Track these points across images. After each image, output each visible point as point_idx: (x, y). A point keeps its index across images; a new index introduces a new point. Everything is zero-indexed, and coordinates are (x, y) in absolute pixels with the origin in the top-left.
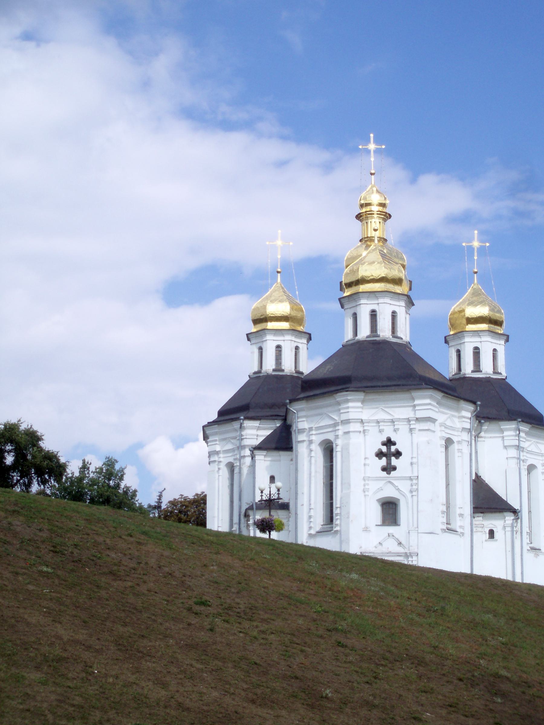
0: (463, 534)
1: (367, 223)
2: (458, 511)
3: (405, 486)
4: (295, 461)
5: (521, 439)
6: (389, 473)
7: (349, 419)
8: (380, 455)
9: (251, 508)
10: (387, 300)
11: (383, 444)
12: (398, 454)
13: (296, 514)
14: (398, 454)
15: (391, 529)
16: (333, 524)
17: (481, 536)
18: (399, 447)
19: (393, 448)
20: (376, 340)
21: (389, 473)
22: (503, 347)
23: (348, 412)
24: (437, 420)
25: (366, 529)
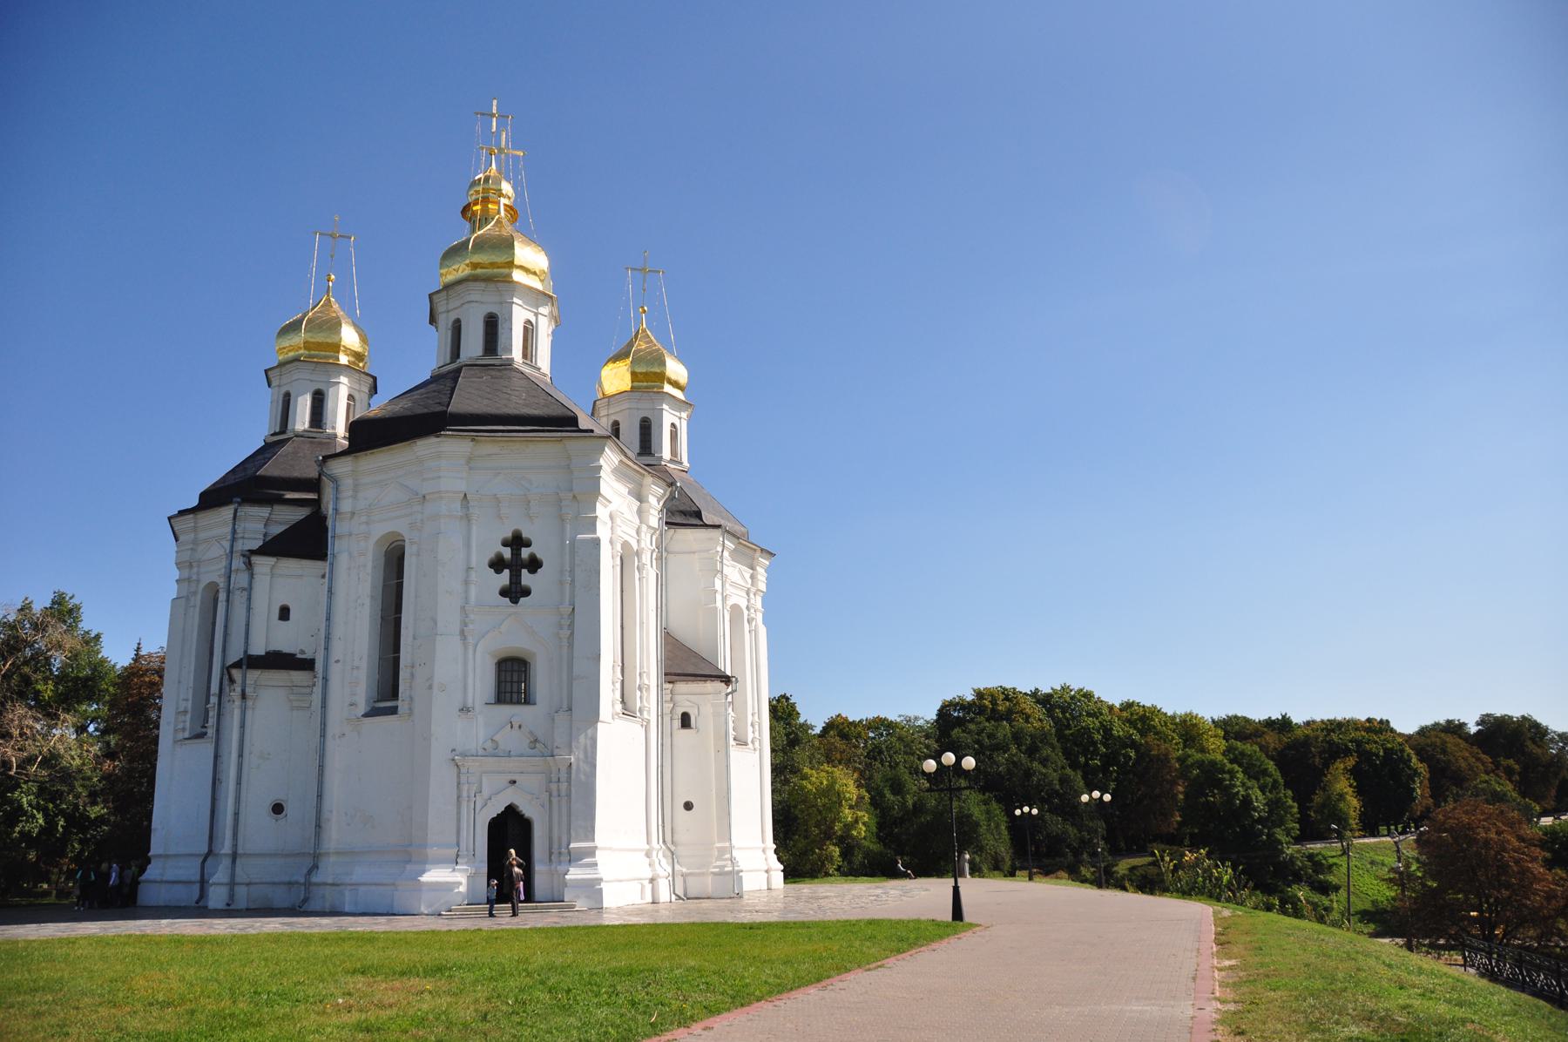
4: (330, 578)
5: (725, 561)
6: (515, 601)
7: (439, 492)
8: (497, 564)
9: (238, 665)
12: (534, 565)
13: (325, 679)
14: (534, 565)
16: (398, 699)
18: (537, 549)
19: (525, 553)
21: (515, 601)
22: (684, 423)
23: (439, 477)
24: (610, 502)
25: (465, 710)
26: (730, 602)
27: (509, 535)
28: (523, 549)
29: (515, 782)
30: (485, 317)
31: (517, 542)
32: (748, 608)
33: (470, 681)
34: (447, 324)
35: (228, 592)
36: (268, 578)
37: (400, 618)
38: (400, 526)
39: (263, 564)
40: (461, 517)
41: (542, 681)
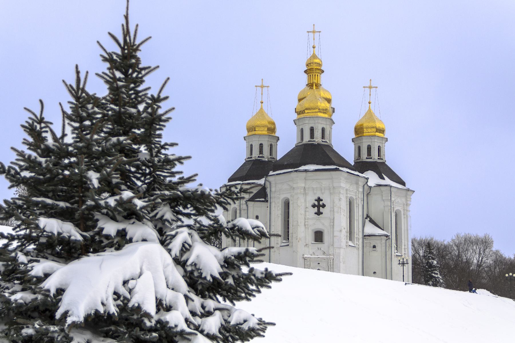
0: (359, 248)
1: (310, 75)
2: (356, 236)
3: (327, 223)
8: (314, 206)
10: (320, 121)
11: (316, 200)
14: (324, 206)
15: (319, 245)
17: (367, 249)
19: (321, 203)
20: (313, 143)
23: (298, 183)
26: (395, 209)
27: (317, 198)
28: (320, 202)
29: (319, 263)
30: (310, 128)
31: (319, 200)
32: (404, 210)
33: (307, 237)
34: (299, 129)
35: (240, 211)
36: (252, 208)
37: (289, 220)
38: (288, 196)
39: (250, 204)
40: (304, 194)
41: (326, 237)
